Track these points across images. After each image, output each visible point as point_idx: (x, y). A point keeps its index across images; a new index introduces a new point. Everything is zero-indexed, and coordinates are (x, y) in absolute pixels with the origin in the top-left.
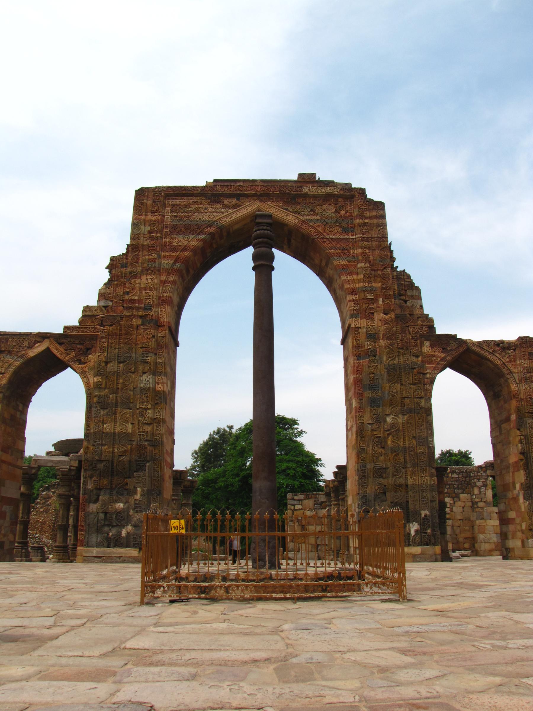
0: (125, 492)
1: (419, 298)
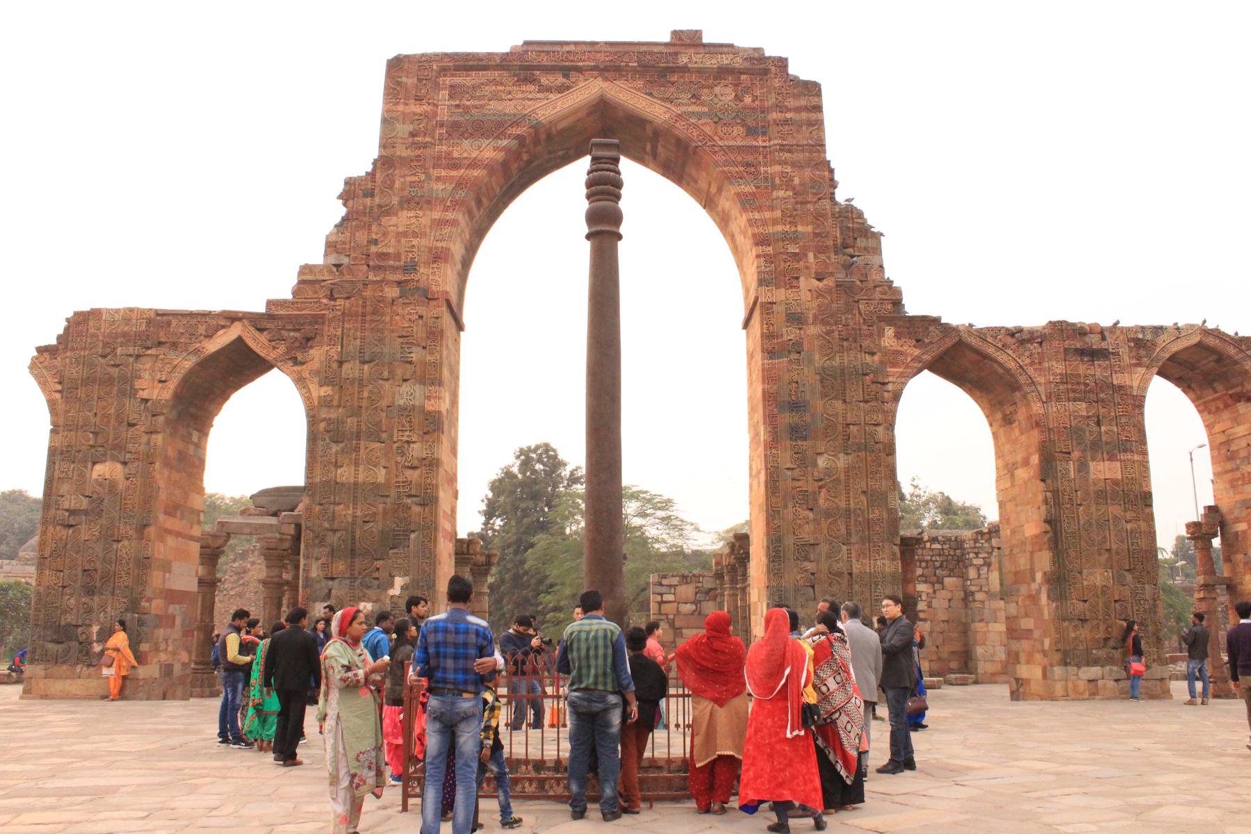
0: (376, 583)
1: (877, 250)
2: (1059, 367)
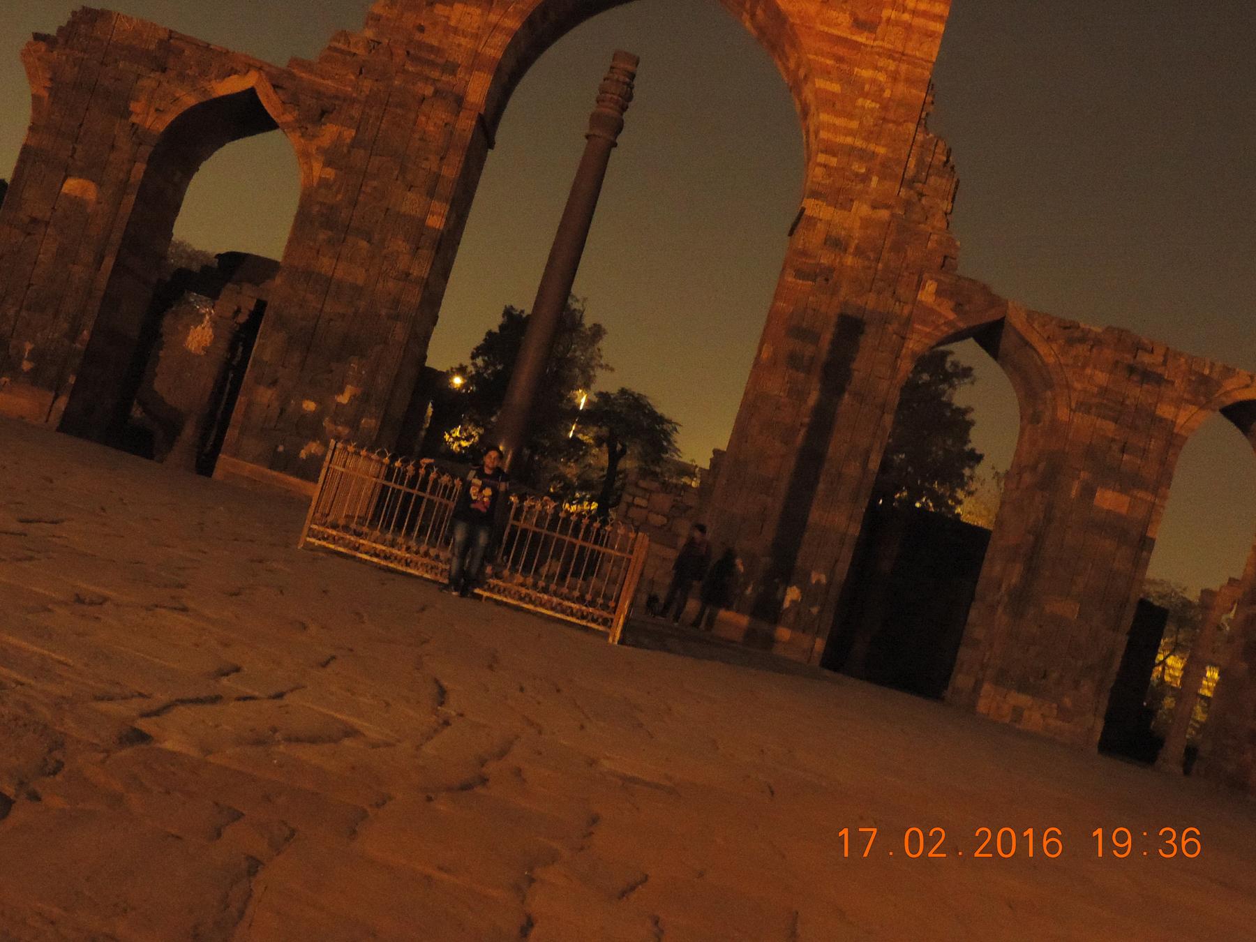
2: (1101, 377)
